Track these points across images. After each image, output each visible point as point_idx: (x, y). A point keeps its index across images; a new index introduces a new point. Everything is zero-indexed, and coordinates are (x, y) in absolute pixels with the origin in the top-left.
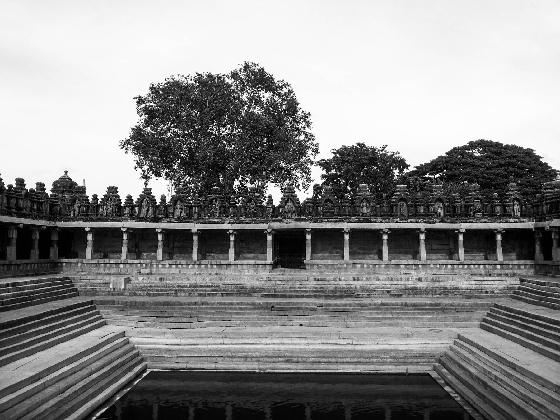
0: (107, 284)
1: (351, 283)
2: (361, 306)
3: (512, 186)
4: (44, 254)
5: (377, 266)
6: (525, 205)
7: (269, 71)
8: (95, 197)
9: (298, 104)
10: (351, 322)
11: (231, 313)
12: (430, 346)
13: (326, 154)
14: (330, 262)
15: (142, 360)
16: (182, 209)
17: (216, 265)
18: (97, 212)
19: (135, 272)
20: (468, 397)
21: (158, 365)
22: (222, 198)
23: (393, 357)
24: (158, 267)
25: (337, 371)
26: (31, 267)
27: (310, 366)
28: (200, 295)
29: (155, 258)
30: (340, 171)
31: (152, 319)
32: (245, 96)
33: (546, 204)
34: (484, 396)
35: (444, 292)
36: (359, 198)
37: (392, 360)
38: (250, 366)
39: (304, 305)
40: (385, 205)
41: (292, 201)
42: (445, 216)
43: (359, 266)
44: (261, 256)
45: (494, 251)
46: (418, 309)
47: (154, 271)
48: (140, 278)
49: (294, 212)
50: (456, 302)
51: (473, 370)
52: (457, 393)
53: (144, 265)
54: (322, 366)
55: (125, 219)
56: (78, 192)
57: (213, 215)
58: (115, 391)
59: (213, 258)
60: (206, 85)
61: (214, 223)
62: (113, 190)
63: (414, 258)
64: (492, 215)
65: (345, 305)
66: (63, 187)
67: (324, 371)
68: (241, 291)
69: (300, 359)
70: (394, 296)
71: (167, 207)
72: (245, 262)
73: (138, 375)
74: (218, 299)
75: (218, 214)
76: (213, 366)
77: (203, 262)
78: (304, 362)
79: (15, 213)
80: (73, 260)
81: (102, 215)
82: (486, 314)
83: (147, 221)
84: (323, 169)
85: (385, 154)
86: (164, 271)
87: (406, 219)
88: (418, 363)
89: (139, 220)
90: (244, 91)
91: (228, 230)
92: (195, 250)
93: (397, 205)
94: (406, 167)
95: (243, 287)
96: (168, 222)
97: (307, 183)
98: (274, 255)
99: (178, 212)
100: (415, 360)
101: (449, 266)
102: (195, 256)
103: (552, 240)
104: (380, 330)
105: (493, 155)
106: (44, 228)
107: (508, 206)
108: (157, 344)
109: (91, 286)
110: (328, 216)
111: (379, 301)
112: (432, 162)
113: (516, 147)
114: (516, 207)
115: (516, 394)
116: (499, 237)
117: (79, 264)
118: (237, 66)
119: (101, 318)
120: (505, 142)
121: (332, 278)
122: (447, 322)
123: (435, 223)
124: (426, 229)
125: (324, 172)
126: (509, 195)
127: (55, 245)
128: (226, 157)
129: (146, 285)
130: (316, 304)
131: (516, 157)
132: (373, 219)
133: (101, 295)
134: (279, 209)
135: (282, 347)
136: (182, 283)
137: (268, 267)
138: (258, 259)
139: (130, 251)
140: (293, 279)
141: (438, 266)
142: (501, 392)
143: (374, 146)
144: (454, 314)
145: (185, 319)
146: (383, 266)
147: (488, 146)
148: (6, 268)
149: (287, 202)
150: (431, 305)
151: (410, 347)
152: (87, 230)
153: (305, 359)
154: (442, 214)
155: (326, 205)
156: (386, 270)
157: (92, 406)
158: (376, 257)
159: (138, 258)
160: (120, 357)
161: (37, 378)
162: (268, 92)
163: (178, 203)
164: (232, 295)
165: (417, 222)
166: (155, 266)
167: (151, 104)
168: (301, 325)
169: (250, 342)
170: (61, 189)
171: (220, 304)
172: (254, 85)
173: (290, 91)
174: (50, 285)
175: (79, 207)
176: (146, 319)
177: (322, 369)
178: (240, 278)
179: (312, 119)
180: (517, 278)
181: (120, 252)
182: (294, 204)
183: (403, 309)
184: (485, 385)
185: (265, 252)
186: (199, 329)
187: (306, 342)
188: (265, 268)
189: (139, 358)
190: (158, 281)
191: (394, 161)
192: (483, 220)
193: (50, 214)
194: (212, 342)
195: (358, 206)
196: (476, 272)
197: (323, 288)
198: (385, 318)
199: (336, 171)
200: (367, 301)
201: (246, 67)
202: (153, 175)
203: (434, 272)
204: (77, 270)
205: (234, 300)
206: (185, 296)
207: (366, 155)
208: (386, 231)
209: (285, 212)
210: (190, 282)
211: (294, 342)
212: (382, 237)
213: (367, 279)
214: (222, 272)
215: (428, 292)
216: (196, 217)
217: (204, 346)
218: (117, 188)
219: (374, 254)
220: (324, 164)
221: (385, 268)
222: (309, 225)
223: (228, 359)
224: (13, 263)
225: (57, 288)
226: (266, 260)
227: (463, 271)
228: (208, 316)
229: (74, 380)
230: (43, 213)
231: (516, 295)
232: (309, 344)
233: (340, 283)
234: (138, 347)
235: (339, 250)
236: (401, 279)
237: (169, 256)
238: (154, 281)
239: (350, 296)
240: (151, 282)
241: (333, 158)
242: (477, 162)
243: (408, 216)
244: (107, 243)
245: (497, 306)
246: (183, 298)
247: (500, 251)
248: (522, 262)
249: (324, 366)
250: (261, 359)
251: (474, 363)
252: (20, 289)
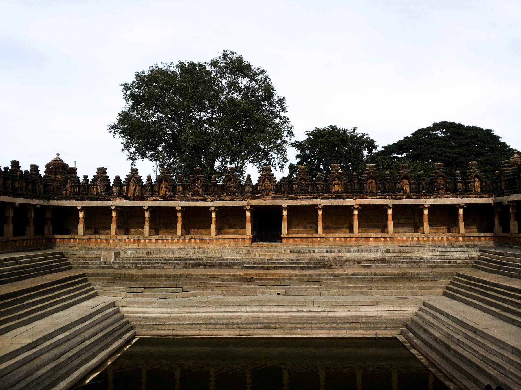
0: (98, 258)
1: (325, 255)
2: (333, 275)
3: (473, 164)
4: (39, 231)
5: (348, 239)
6: (485, 182)
7: (246, 59)
8: (86, 177)
9: (273, 90)
10: (324, 291)
11: (213, 284)
12: (398, 312)
13: (301, 136)
14: (304, 236)
15: (132, 328)
16: (167, 188)
17: (199, 239)
18: (88, 191)
19: (124, 247)
20: (433, 359)
21: (145, 332)
22: (204, 177)
23: (364, 323)
24: (145, 242)
25: (312, 336)
26: (26, 243)
27: (286, 331)
28: (185, 267)
29: (142, 233)
30: (313, 152)
31: (139, 290)
32: (224, 83)
33: (504, 180)
34: (447, 358)
35: (411, 262)
36: (331, 176)
37: (363, 326)
38: (232, 332)
39: (281, 275)
40: (355, 183)
41: (269, 180)
42: (411, 192)
43: (331, 239)
44: (241, 231)
45: (457, 224)
46: (386, 279)
47: (141, 245)
48: (129, 253)
49: (271, 190)
50: (421, 272)
51: (437, 334)
52: (422, 355)
53: (132, 240)
54: (298, 331)
55: (114, 198)
56: (70, 173)
57: (195, 193)
58: (106, 357)
59: (196, 233)
60: (188, 73)
61: (197, 200)
62: (102, 171)
63: (383, 231)
64: (454, 192)
65: (319, 275)
66: (56, 169)
67: (300, 336)
68: (223, 263)
69: (277, 326)
70: (364, 267)
71: (152, 186)
72: (226, 236)
73: (128, 342)
74: (201, 271)
75: (200, 192)
76: (197, 332)
77: (187, 237)
78: (281, 328)
79: (11, 193)
81: (93, 194)
82: (449, 282)
83: (134, 200)
84: (298, 150)
85: (356, 136)
86: (151, 245)
87: (375, 196)
88: (386, 328)
89: (127, 198)
90: (223, 77)
91: (210, 207)
92: (179, 226)
93: (366, 183)
94: (375, 147)
95: (224, 260)
96: (154, 200)
97: (283, 163)
98: (254, 229)
99: (163, 191)
100: (384, 326)
101: (415, 239)
102: (179, 231)
103: (510, 213)
104: (350, 298)
105: (455, 136)
107: (470, 182)
108: (145, 313)
109: (83, 260)
110: (302, 193)
111: (350, 272)
112: (399, 142)
113: (477, 128)
114: (477, 184)
115: (477, 355)
116: (461, 211)
117: (72, 240)
118: (216, 55)
119: (93, 289)
120: (467, 122)
121: (307, 251)
122: (413, 290)
123: (402, 199)
124: (393, 205)
125: (299, 153)
126: (470, 172)
127: (49, 223)
128: (207, 139)
129: (134, 259)
130: (292, 275)
131: (477, 137)
132: (344, 196)
133: (93, 268)
134: (257, 187)
135: (261, 315)
136: (168, 257)
137: (247, 241)
138: (238, 234)
139: (119, 227)
140: (270, 252)
141: (405, 239)
142: (463, 354)
143: (345, 128)
144: (419, 282)
145: (170, 290)
146: (354, 239)
147: (451, 127)
149: (264, 180)
150: (398, 274)
151: (379, 314)
152: (79, 208)
153: (282, 326)
154: (408, 191)
155: (301, 183)
156: (356, 242)
157: (86, 371)
158: (348, 231)
159: (127, 233)
160: (110, 325)
161: (34, 345)
162: (246, 79)
163: (163, 182)
164: (214, 267)
165: (385, 198)
166: (142, 241)
167: (137, 90)
168: (278, 294)
169: (231, 310)
170: (54, 170)
171: (203, 275)
172: (232, 72)
173: (266, 78)
174: (45, 259)
175: (71, 187)
176: (135, 290)
177: (298, 334)
178: (221, 252)
179: (287, 103)
180: (478, 249)
181: (110, 228)
182: (271, 182)
183: (372, 278)
184: (448, 348)
185: (244, 227)
186: (185, 299)
187: (283, 309)
188: (245, 242)
189: (129, 326)
190: (145, 255)
191: (364, 141)
192: (446, 196)
193: (44, 193)
194: (196, 311)
195: (330, 184)
196: (440, 243)
197: (298, 260)
198: (357, 287)
199: (310, 152)
200: (340, 271)
201: (225, 55)
202: (139, 157)
203: (401, 245)
204: (70, 245)
205: (216, 272)
206: (170, 269)
207: (338, 136)
208: (357, 207)
209: (263, 190)
210: (175, 255)
211: (272, 310)
212: (353, 212)
213: (339, 251)
214: (205, 246)
215: (395, 263)
216: (180, 195)
217: (189, 315)
218: (106, 169)
219: (346, 228)
220: (298, 145)
221: (356, 241)
222: (285, 202)
223: (211, 326)
224: (10, 239)
225: (51, 262)
226: (246, 234)
227: (427, 244)
228: (192, 287)
229: (68, 347)
230: (37, 192)
231: (476, 264)
232: (285, 312)
233: (315, 255)
234: (128, 316)
235: (313, 225)
236: (371, 251)
237: (155, 232)
238: (141, 255)
239: (324, 267)
240: (139, 256)
241: (307, 139)
242: (441, 142)
243: (377, 193)
244: (97, 220)
245: (459, 275)
246: (169, 271)
247: (461, 224)
248: (482, 234)
249: (300, 331)
250: (241, 326)
251: (438, 327)
252: (17, 264)
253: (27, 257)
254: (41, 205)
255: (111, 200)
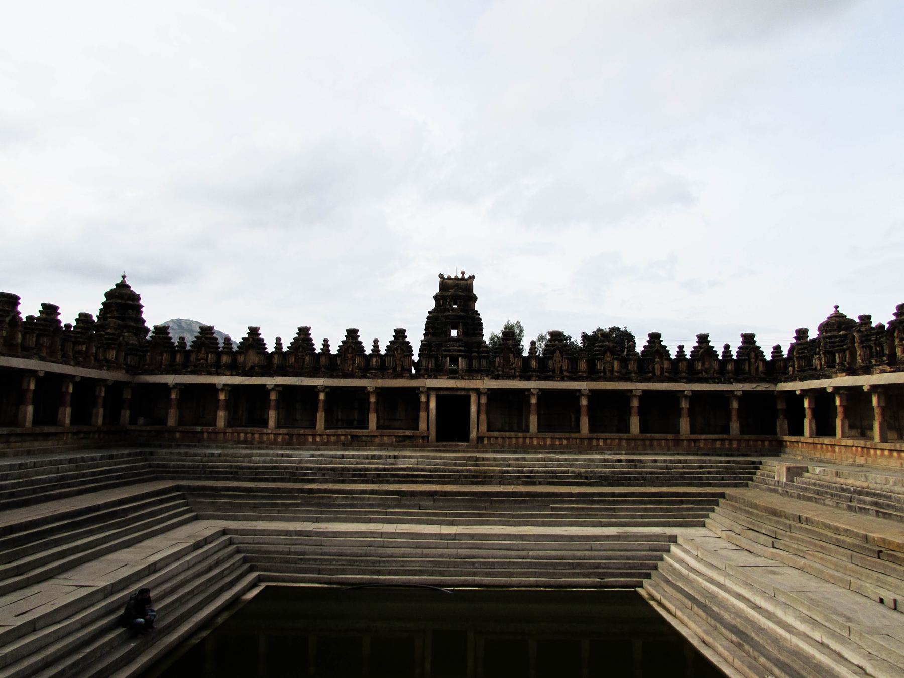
24: (875, 453)
26: (722, 444)
47: (869, 458)
79: (683, 378)
80: (793, 439)
86: (882, 462)
89: (851, 372)
106: (740, 393)
127: (781, 417)
148: (671, 444)
174: (701, 467)
224: (683, 438)
225: (709, 472)
252: (636, 467)
253: (665, 461)
254: (744, 392)
255: (831, 377)
